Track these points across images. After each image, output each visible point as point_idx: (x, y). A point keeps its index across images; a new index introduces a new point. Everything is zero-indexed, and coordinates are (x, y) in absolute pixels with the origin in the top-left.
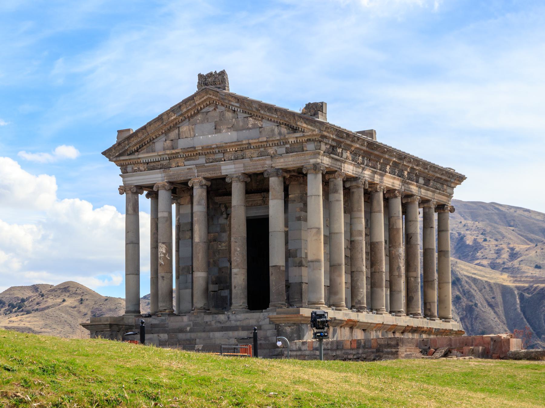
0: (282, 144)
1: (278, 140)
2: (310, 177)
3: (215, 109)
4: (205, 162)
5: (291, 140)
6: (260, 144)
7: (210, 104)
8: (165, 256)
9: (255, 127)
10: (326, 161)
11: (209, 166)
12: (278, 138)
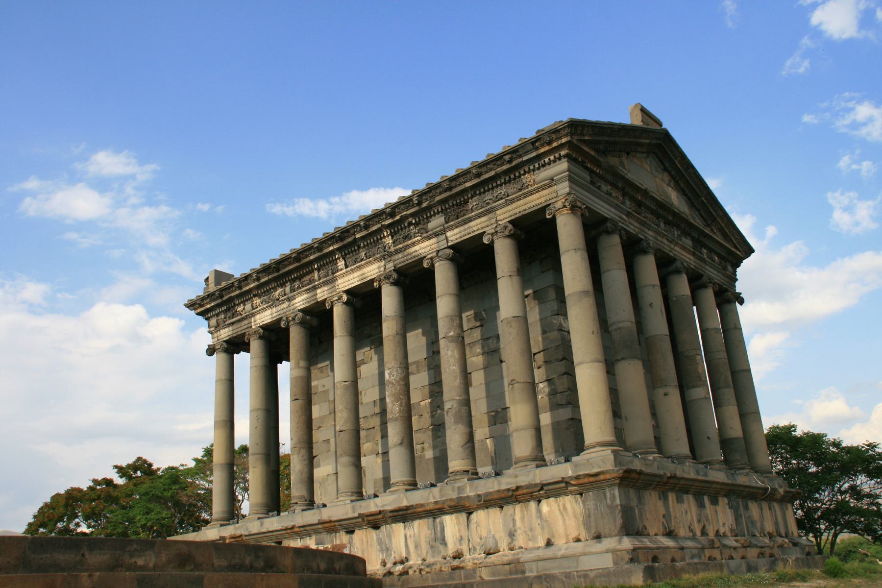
10: (225, 333)
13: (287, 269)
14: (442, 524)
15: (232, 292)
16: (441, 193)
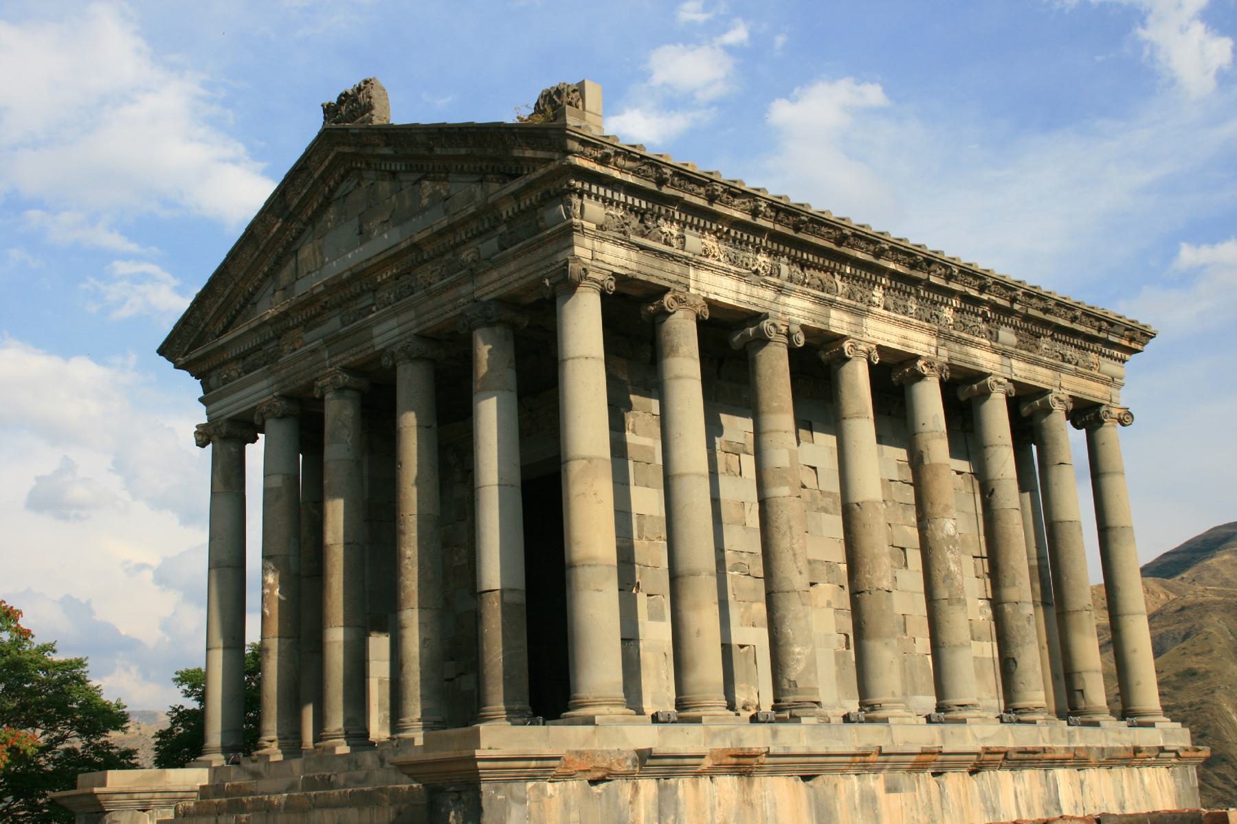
1: (474, 216)
5: (507, 210)
7: (348, 172)
10: (617, 258)
11: (347, 335)
12: (472, 210)
13: (813, 240)
14: (1055, 780)
15: (691, 192)
16: (1037, 309)
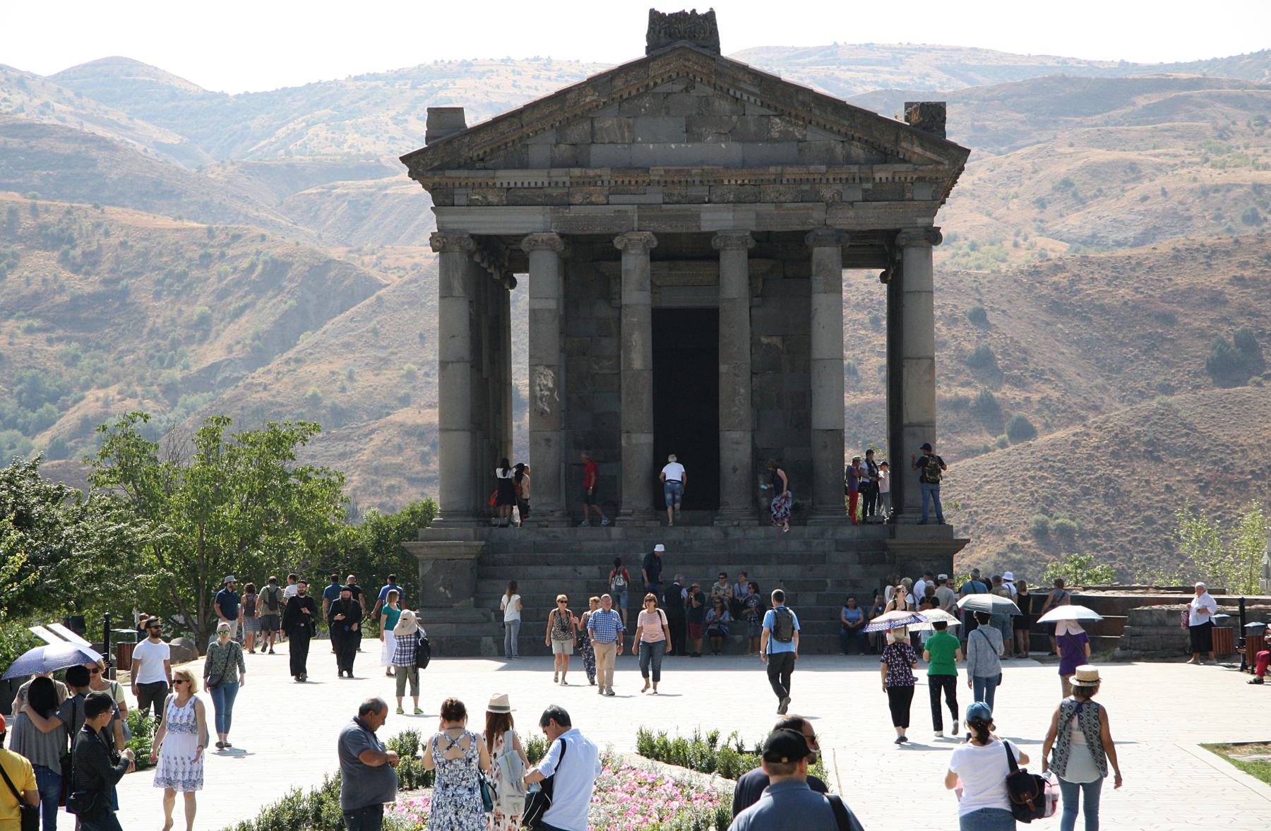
0: (857, 180)
2: (912, 256)
3: (686, 90)
4: (659, 199)
6: (804, 177)
8: (552, 395)
9: (786, 137)
